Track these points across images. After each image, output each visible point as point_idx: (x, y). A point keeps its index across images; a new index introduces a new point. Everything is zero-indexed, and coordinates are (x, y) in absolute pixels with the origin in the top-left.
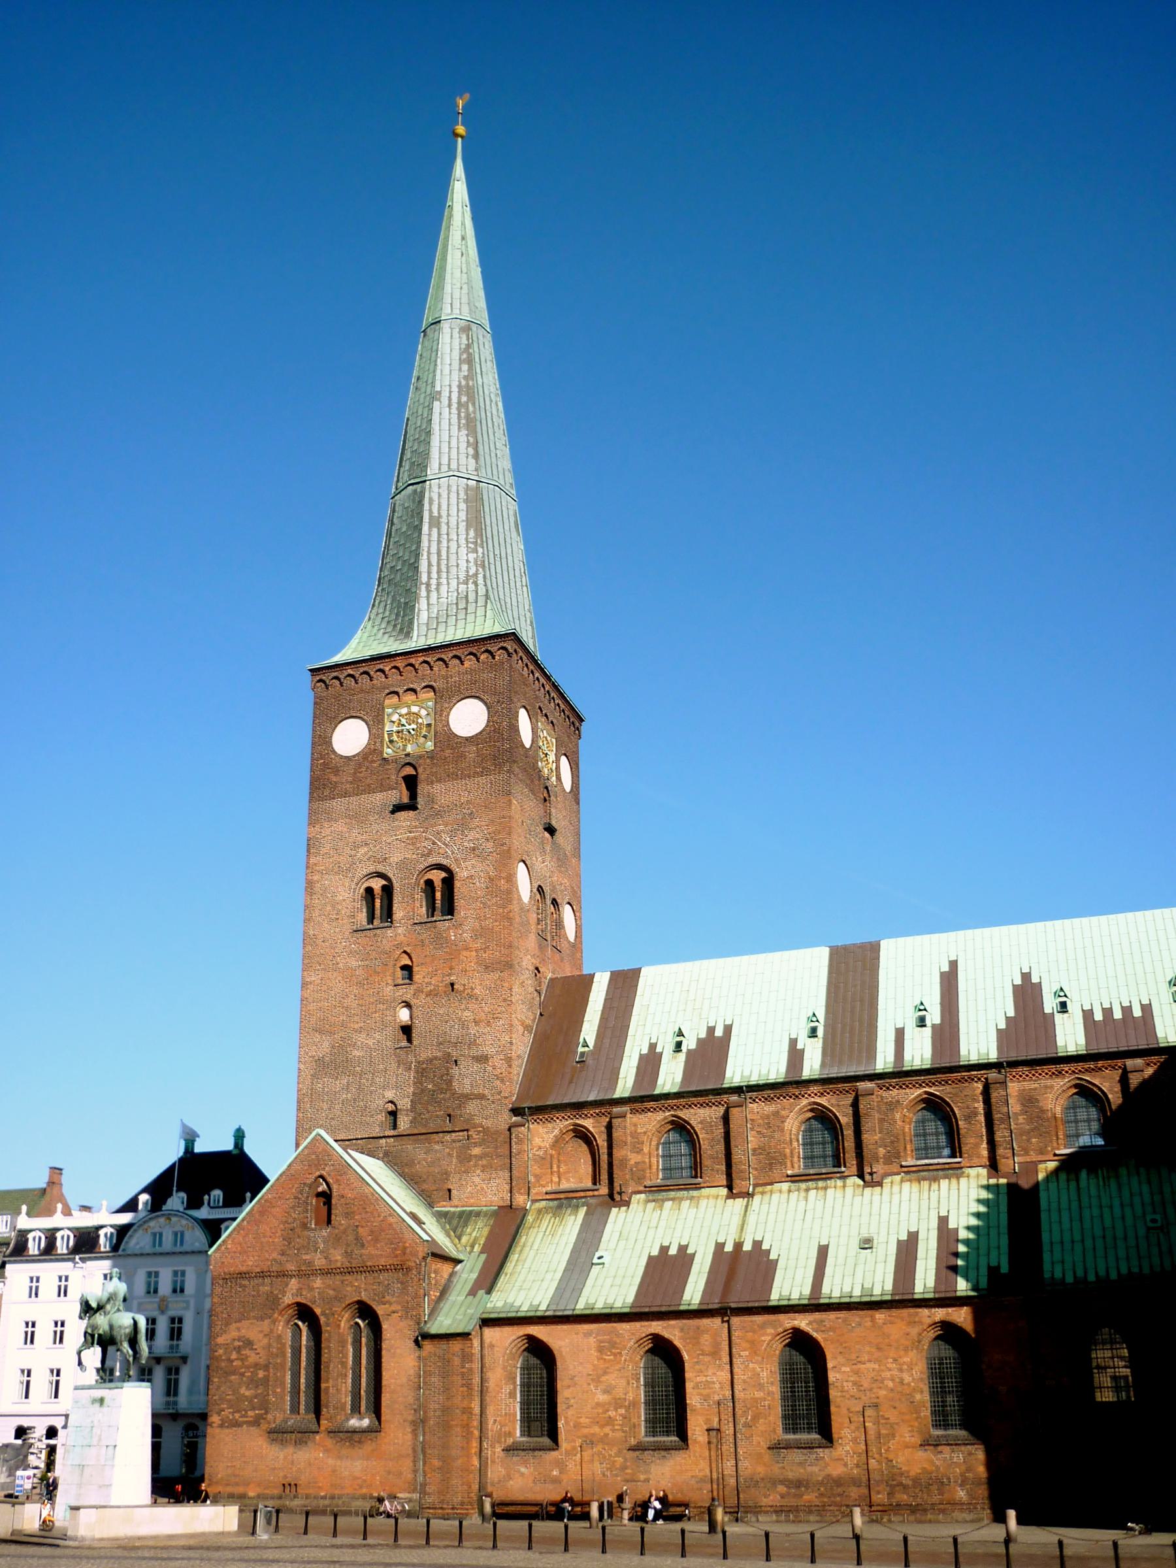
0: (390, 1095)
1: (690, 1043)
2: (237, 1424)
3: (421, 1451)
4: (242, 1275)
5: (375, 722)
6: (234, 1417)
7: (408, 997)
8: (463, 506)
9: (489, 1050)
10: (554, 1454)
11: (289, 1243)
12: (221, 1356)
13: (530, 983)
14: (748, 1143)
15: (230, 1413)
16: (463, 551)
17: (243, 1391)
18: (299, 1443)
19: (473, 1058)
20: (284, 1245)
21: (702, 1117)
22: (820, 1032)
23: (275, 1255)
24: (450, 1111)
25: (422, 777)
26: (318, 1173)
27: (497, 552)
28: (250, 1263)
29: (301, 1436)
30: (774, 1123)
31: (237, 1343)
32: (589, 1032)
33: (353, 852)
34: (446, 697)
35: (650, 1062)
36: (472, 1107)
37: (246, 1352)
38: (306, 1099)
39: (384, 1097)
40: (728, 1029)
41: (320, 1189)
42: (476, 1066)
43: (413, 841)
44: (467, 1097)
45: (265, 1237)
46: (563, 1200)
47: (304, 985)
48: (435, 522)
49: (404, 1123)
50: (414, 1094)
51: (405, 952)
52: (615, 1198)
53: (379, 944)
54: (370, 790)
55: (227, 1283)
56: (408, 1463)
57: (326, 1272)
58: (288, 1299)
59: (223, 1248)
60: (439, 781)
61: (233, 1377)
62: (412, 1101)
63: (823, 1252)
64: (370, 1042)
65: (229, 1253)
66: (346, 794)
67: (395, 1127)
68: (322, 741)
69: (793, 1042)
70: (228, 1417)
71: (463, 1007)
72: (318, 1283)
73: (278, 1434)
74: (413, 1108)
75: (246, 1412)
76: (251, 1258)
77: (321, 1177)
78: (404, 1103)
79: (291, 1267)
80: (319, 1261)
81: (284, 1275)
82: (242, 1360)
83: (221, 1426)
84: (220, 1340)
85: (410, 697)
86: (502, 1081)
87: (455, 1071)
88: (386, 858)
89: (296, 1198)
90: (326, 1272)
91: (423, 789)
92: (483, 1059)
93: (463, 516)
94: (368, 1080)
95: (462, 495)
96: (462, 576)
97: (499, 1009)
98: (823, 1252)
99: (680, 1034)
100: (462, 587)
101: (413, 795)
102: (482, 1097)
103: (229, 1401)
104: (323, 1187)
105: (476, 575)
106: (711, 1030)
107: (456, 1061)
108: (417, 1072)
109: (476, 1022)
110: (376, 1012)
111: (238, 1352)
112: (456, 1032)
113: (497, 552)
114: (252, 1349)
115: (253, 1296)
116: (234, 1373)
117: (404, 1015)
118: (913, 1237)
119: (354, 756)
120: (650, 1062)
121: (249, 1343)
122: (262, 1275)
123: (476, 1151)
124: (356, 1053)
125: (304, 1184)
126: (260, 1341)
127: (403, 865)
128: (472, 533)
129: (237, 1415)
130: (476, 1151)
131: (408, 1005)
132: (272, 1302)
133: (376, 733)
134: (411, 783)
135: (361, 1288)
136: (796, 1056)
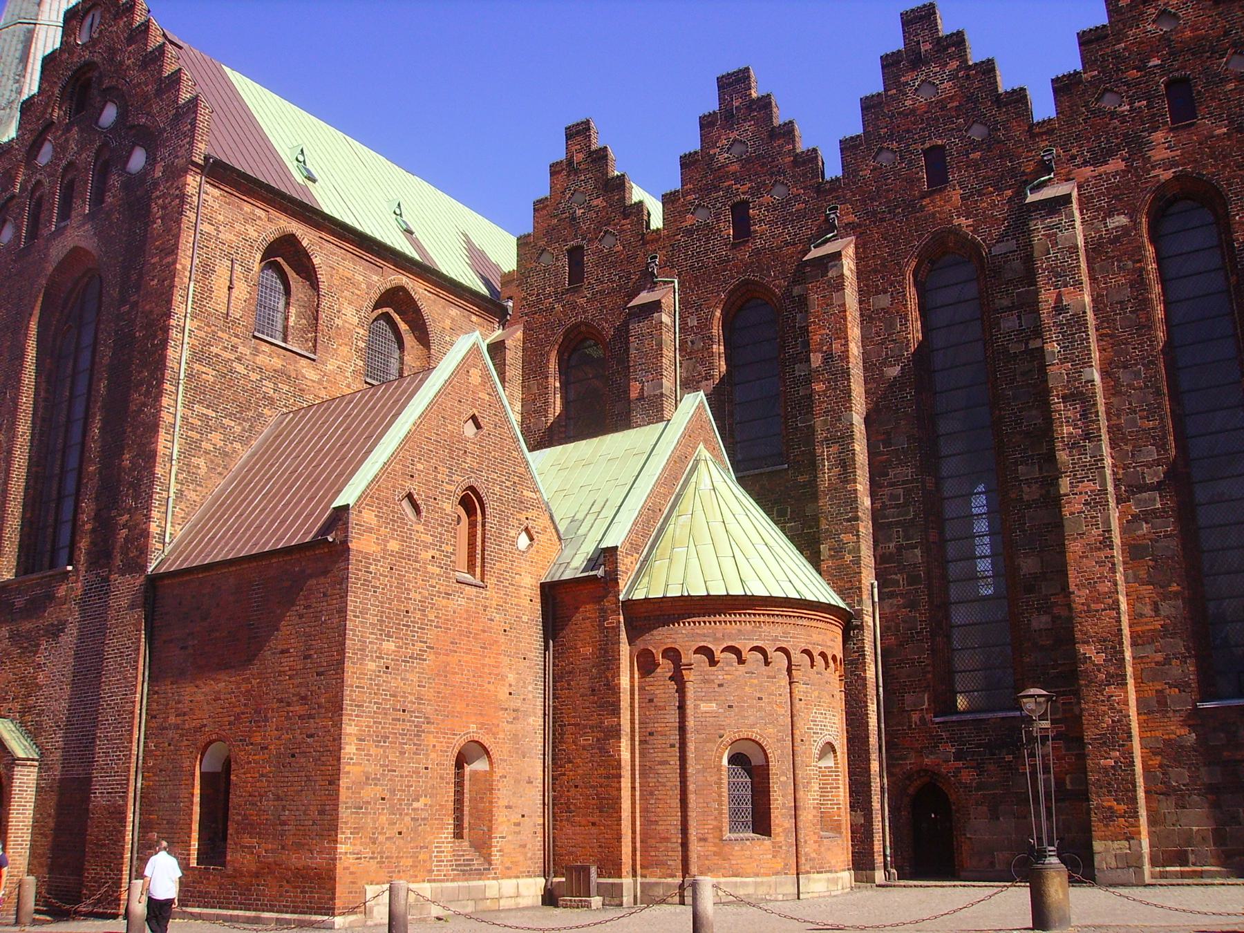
8: (20, 47)
16: (11, 82)
93: (18, 54)
95: (22, 38)
105: (13, 102)
128: (20, 68)
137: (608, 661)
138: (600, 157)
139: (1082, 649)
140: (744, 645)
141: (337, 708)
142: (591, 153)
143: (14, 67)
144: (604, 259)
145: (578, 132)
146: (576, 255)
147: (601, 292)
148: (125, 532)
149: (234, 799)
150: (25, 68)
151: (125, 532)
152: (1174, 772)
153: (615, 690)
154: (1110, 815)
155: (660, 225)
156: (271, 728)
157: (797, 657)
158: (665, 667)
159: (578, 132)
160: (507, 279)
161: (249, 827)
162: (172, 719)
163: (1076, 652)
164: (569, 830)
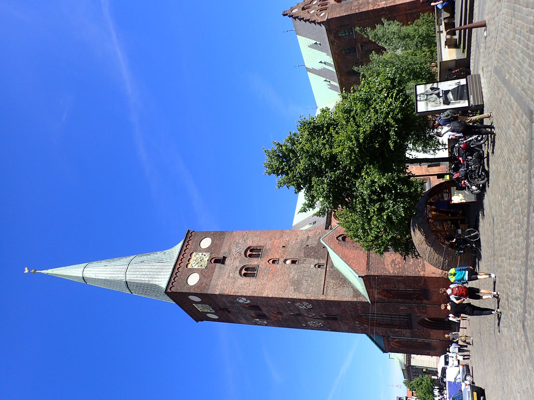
0: (312, 266)
5: (193, 271)
6: (421, 266)
7: (283, 260)
9: (306, 236)
11: (358, 247)
12: (397, 271)
15: (419, 268)
17: (411, 263)
19: (307, 240)
20: (359, 250)
23: (362, 253)
24: (322, 247)
26: (336, 239)
28: (364, 261)
31: (393, 265)
33: (230, 278)
37: (396, 262)
38: (307, 295)
39: (313, 268)
41: (341, 239)
42: (310, 240)
43: (235, 258)
45: (355, 256)
49: (323, 262)
50: (314, 258)
51: (268, 261)
53: (263, 269)
55: (370, 270)
59: (357, 271)
60: (220, 251)
61: (406, 267)
62: (316, 259)
64: (294, 272)
65: (359, 269)
70: (421, 269)
71: (291, 243)
74: (319, 259)
75: (419, 262)
76: (362, 261)
77: (337, 238)
82: (399, 263)
83: (424, 271)
84: (391, 272)
86: (316, 232)
87: (310, 246)
88: (237, 267)
89: (342, 246)
92: (308, 237)
94: (306, 273)
97: (295, 233)
103: (415, 268)
104: (340, 238)
107: (307, 246)
108: (307, 258)
109: (297, 239)
110: (284, 271)
111: (396, 265)
112: (298, 246)
114: (395, 260)
115: (376, 260)
116: (404, 267)
117: (288, 262)
119: (200, 277)
121: (393, 261)
124: (296, 278)
125: (338, 243)
126: (392, 257)
127: (240, 262)
129: (420, 265)
131: (285, 261)
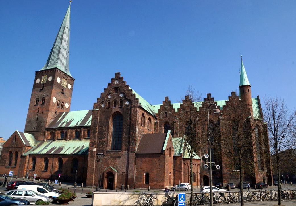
0: (34, 126)
1: (68, 121)
2: (2, 166)
3: (19, 170)
4: (6, 147)
9: (45, 121)
10: (34, 171)
13: (54, 113)
14: (69, 134)
18: (8, 168)
21: (65, 131)
22: (82, 121)
25: (44, 85)
27: (62, 57)
29: (8, 168)
30: (72, 132)
32: (59, 120)
34: (48, 76)
35: (63, 123)
36: (42, 128)
40: (73, 119)
42: (43, 123)
44: (42, 127)
46: (49, 140)
47: (28, 112)
48: (54, 53)
49: (35, 130)
52: (54, 140)
54: (39, 88)
56: (18, 171)
57: (14, 147)
58: (10, 151)
63: (69, 148)
66: (36, 88)
67: (34, 130)
68: (35, 81)
69: (78, 122)
72: (13, 149)
73: (6, 167)
78: (35, 127)
79: (11, 147)
80: (14, 146)
81: (10, 148)
85: (45, 76)
90: (14, 147)
91: (44, 87)
92: (44, 122)
93: (58, 52)
95: (58, 50)
96: (55, 60)
98: (69, 148)
99: (68, 120)
100: (55, 62)
101: (43, 88)
102: (43, 127)
106: (71, 120)
113: (62, 57)
118: (79, 147)
120: (63, 123)
122: (8, 147)
123: (42, 134)
127: (40, 97)
130: (42, 134)
132: (8, 150)
133: (40, 81)
134: (43, 86)
135: (17, 150)
136: (78, 123)
137: (181, 164)
138: (170, 102)
139: (223, 165)
140: (194, 163)
141: (164, 170)
142: (168, 101)
143: (57, 54)
144: (170, 114)
145: (167, 98)
146: (166, 113)
147: (169, 118)
148: (131, 148)
149: (150, 178)
150: (59, 55)
151: (131, 148)
152: (230, 177)
153: (182, 167)
154: (224, 181)
155: (177, 112)
156: (155, 171)
157: (198, 165)
158: (187, 165)
159: (167, 98)
160: (157, 114)
161: (152, 181)
162: (140, 169)
163: (222, 165)
164: (176, 181)
